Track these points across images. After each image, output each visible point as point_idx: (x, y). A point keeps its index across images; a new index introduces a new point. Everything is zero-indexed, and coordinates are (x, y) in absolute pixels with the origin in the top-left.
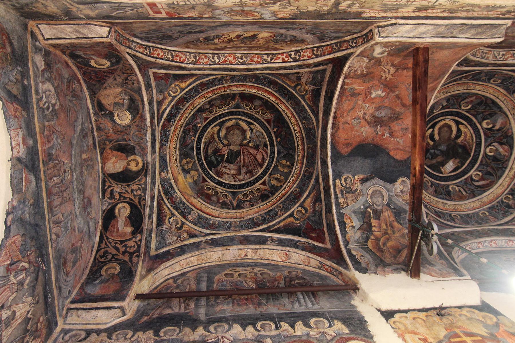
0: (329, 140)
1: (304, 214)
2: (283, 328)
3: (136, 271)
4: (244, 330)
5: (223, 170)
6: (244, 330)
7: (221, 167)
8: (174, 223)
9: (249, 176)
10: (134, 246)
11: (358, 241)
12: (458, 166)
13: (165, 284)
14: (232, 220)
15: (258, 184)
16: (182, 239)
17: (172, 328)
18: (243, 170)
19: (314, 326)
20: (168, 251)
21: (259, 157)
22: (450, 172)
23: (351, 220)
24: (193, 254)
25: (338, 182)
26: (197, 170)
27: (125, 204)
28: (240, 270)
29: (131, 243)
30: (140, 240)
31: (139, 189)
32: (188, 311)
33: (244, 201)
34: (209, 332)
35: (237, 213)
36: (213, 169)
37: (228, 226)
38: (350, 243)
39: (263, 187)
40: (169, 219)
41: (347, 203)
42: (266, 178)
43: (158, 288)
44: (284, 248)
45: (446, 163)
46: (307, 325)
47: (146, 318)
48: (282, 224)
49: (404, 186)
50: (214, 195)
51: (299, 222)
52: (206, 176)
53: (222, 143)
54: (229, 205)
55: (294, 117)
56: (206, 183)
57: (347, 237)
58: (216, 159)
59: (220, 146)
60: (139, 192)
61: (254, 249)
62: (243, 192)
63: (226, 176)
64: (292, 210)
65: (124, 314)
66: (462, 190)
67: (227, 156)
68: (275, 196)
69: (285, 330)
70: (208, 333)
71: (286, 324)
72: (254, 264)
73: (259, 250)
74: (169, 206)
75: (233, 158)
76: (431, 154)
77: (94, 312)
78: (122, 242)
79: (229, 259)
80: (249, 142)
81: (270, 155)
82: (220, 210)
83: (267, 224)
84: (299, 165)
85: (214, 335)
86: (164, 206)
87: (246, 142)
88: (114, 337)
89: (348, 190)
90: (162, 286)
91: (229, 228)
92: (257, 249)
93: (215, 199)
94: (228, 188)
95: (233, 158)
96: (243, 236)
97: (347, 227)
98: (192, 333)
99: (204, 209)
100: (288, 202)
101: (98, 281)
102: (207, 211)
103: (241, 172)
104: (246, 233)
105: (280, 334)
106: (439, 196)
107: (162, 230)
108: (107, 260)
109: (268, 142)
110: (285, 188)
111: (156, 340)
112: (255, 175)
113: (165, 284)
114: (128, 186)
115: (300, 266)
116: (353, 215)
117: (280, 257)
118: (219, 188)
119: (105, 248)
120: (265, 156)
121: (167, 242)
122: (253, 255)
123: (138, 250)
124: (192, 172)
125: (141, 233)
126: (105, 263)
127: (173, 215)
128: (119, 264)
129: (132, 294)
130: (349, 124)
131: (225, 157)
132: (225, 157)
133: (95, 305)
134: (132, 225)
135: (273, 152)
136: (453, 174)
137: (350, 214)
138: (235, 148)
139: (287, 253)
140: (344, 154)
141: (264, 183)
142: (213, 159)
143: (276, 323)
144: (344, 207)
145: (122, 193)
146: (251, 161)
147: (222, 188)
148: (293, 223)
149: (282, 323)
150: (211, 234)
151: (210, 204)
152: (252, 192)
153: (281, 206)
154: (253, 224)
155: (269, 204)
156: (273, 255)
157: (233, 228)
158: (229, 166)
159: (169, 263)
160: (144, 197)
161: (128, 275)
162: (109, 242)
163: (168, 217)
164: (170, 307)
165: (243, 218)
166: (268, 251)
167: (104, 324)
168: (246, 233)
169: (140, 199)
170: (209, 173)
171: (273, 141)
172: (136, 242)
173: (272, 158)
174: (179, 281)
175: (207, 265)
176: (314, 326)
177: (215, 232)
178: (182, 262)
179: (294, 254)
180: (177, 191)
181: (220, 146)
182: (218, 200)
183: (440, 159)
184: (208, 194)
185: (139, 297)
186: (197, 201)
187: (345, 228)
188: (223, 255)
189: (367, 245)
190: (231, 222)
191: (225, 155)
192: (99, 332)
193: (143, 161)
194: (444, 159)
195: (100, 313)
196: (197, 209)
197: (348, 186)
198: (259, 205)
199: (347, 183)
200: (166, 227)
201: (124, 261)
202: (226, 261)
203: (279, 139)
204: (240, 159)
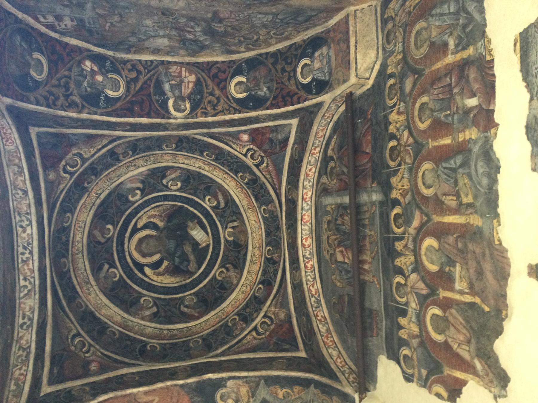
12: (197, 223)
22: (207, 233)
45: (194, 239)
49: (229, 397)
66: (231, 225)
76: (181, 263)
106: (241, 265)
136: (209, 230)
183: (188, 249)
194: (188, 243)
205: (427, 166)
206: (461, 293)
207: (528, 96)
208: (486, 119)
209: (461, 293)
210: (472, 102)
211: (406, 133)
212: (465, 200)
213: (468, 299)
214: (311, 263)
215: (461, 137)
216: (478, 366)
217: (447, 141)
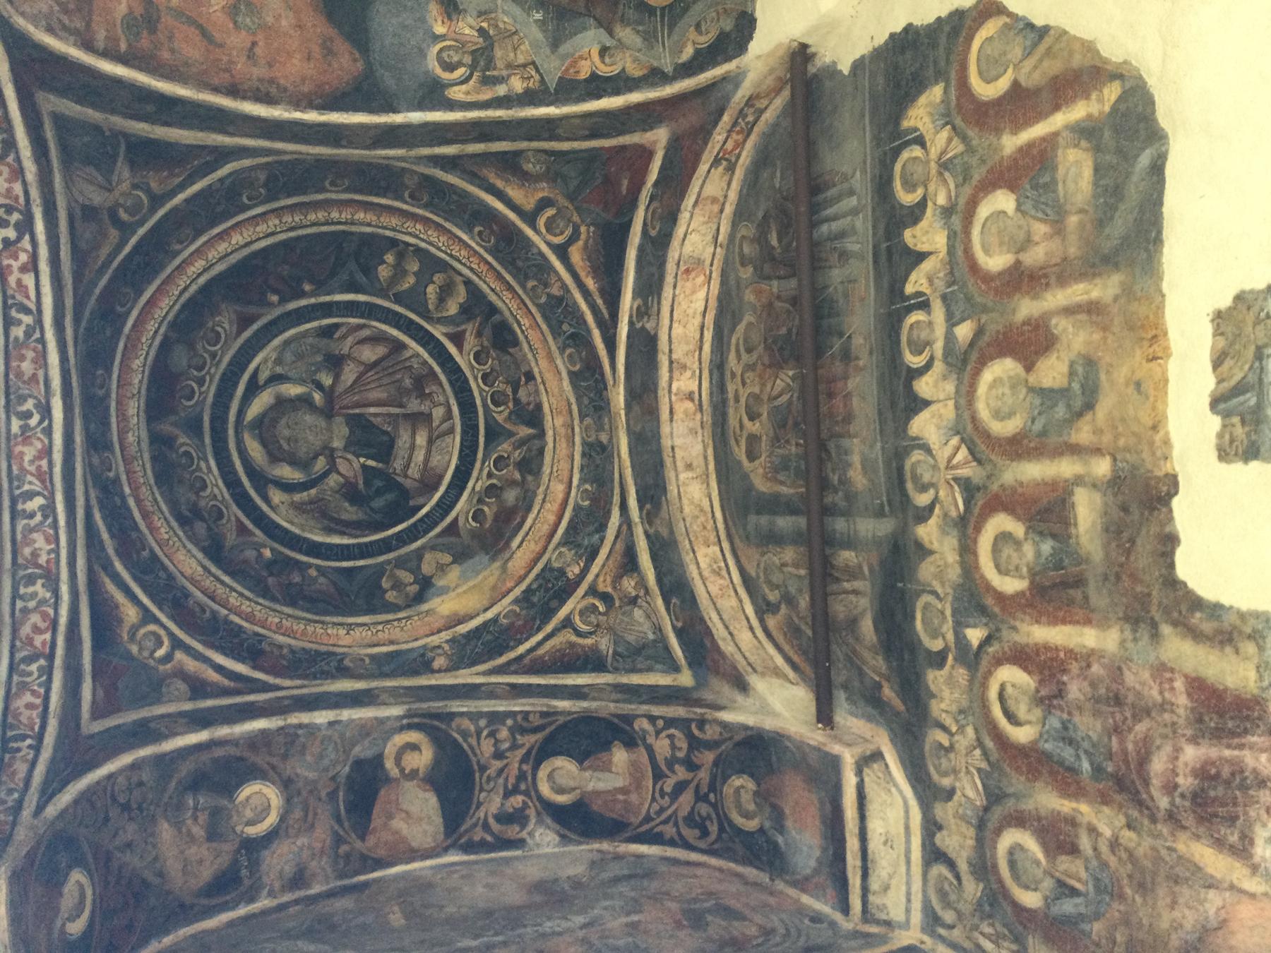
0: (312, 116)
1: (559, 210)
2: (925, 288)
3: (746, 728)
4: (927, 403)
5: (414, 472)
6: (927, 403)
7: (406, 476)
8: (593, 619)
9: (434, 388)
10: (671, 737)
11: (650, 38)
13: (780, 639)
14: (578, 439)
15: (458, 359)
16: (642, 593)
17: (919, 616)
18: (414, 405)
19: (920, 192)
20: (679, 633)
21: (369, 354)
23: (581, 58)
24: (688, 558)
25: (457, 93)
26: (419, 554)
27: (542, 774)
28: (735, 415)
29: (662, 746)
30: (652, 719)
31: (492, 734)
32: (866, 569)
33: (517, 401)
34: (931, 508)
35: (553, 423)
36: (411, 503)
37: (597, 457)
38: (655, 64)
39: (470, 342)
40: (579, 634)
41: (525, 66)
42: (438, 332)
43: (796, 658)
44: (669, 279)
46: (915, 214)
47: (888, 692)
48: (590, 283)
50: (498, 497)
51: (583, 229)
52: (436, 524)
53: (325, 475)
54: (529, 450)
55: (226, 232)
56: (461, 522)
57: (638, 73)
58: (379, 493)
59: (333, 480)
60: (504, 733)
61: (671, 371)
62: (485, 405)
63: (436, 460)
64: (544, 248)
65: (877, 756)
67: (368, 457)
68: (500, 304)
69: (931, 281)
70: (937, 511)
71: (913, 277)
72: (715, 371)
73: (674, 356)
74: (540, 636)
75: (373, 440)
77: (874, 844)
78: (658, 776)
79: (699, 447)
80: (319, 386)
81: (362, 317)
82: (545, 478)
83: (589, 331)
84: (394, 221)
85: (942, 493)
86: (541, 652)
87: (317, 397)
88: (946, 782)
89: (482, 59)
90: (787, 648)
91: (603, 448)
92: (671, 362)
93: (511, 496)
94: (475, 453)
95: (373, 440)
96: (628, 407)
97: (605, 70)
98: (937, 556)
99: (545, 529)
100: (520, 263)
101: (780, 840)
102: (552, 518)
103: (422, 414)
104: (618, 397)
105: (944, 298)
107: (615, 653)
108: (714, 816)
109: (315, 324)
110: (471, 269)
111: (955, 659)
112: (431, 368)
113: (780, 639)
114: (483, 769)
115: (722, 230)
116: (565, 48)
117: (694, 292)
118: (477, 483)
119: (676, 824)
120: (366, 333)
121: (651, 636)
122: (688, 373)
123: (682, 724)
124: (427, 568)
125: (629, 719)
126: (724, 820)
127: (567, 623)
128: (725, 779)
129: (816, 736)
130: (254, 44)
131: (371, 463)
132: (371, 463)
133: (852, 844)
134: (606, 746)
135: (351, 308)
137: (563, 58)
138: (339, 435)
139: (683, 268)
140: (360, 65)
141: (458, 339)
142: (378, 503)
143: (909, 310)
144: (537, 77)
145: (506, 786)
146: (385, 381)
147: (475, 474)
148: (586, 247)
149: (909, 289)
150: (624, 506)
151: (529, 509)
152: (485, 377)
153: (530, 284)
154: (589, 380)
155: (525, 322)
156: (690, 311)
157: (604, 438)
158: (401, 453)
159: (719, 631)
160: (519, 718)
161: (758, 751)
162: (659, 813)
163: (574, 638)
164: (853, 623)
165: (569, 405)
166: (678, 330)
167: (907, 812)
168: (618, 397)
169: (523, 731)
170: (427, 515)
171: (313, 306)
172: (658, 733)
173: (370, 311)
174: (773, 596)
175: (719, 515)
176: (920, 192)
177: (617, 491)
178: (714, 589)
179: (688, 249)
180: (490, 615)
181: (333, 480)
182: (513, 483)
184: (496, 518)
185: (825, 716)
186: (522, 551)
187: (608, 79)
188: (689, 467)
189: (663, 9)
190: (584, 443)
191: (364, 466)
192: (931, 827)
193: (402, 729)
195: (876, 827)
196: (545, 548)
197: (468, 59)
198: (530, 356)
199: (459, 64)
200: (605, 644)
201: (716, 763)
202: (706, 458)
203: (307, 287)
204: (376, 415)
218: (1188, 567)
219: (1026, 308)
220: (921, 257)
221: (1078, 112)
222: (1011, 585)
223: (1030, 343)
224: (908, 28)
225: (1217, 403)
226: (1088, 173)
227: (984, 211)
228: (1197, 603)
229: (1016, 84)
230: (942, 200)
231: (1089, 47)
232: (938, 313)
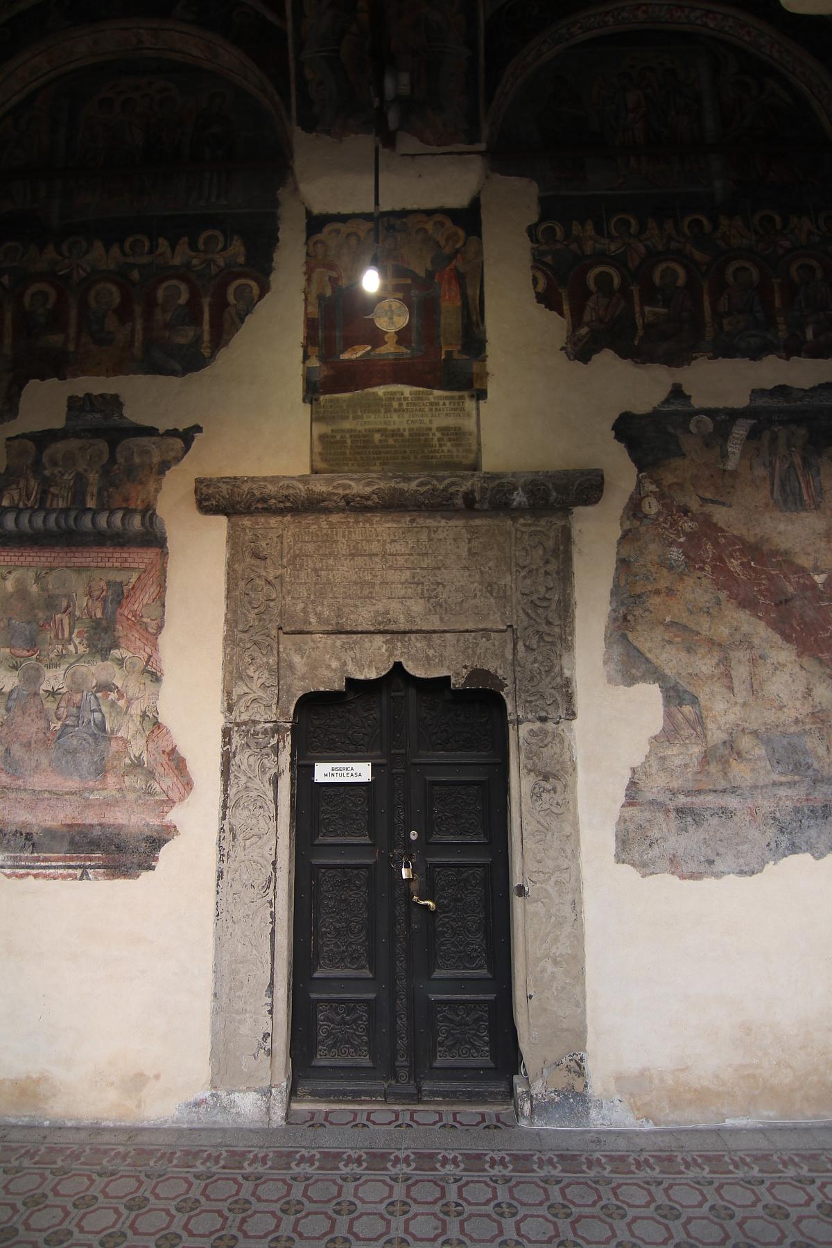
2: (160, 250)
4: (107, 251)
6: (107, 251)
69: (162, 254)
71: (166, 243)
149: (161, 240)
205: (755, 275)
206: (643, 313)
207: (807, 387)
208: (792, 349)
209: (643, 313)
210: (810, 335)
211: (787, 244)
212: (725, 321)
213: (639, 322)
214: (611, 20)
215: (780, 319)
216: (584, 331)
217: (777, 304)
218: (33, 383)
219: (138, 309)
220: (173, 247)
221: (206, 337)
222: (27, 300)
223: (124, 312)
224: (277, 240)
225: (88, 395)
226: (182, 341)
227: (183, 287)
228: (21, 388)
229: (228, 304)
230: (195, 262)
231: (227, 343)
232: (145, 260)
